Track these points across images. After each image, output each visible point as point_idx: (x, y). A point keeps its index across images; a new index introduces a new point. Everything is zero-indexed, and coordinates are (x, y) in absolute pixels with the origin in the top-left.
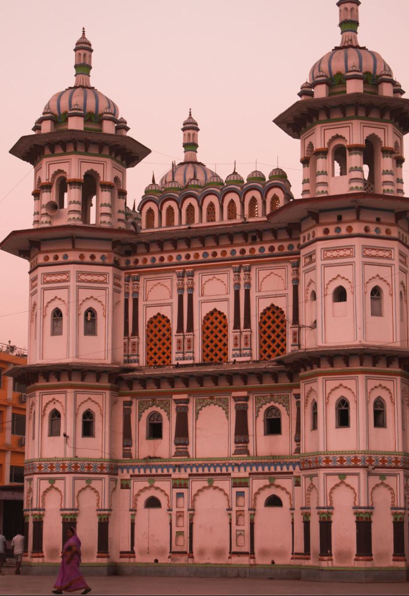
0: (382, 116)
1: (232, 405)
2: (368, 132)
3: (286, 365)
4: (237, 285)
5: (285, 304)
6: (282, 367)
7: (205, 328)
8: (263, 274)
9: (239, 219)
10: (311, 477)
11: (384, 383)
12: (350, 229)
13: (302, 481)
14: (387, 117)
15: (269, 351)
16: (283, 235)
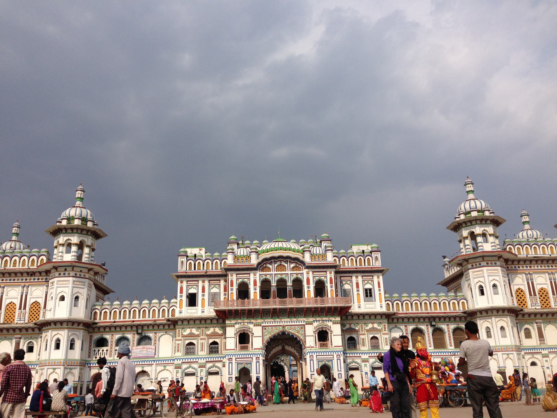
0: (87, 233)
1: (14, 341)
2: (81, 239)
3: (38, 325)
4: (22, 293)
5: (41, 301)
6: (36, 326)
7: (6, 309)
8: (34, 288)
9: (26, 267)
10: (42, 369)
11: (75, 333)
12: (69, 274)
13: (39, 371)
14: (89, 234)
15: (32, 319)
16: (44, 274)
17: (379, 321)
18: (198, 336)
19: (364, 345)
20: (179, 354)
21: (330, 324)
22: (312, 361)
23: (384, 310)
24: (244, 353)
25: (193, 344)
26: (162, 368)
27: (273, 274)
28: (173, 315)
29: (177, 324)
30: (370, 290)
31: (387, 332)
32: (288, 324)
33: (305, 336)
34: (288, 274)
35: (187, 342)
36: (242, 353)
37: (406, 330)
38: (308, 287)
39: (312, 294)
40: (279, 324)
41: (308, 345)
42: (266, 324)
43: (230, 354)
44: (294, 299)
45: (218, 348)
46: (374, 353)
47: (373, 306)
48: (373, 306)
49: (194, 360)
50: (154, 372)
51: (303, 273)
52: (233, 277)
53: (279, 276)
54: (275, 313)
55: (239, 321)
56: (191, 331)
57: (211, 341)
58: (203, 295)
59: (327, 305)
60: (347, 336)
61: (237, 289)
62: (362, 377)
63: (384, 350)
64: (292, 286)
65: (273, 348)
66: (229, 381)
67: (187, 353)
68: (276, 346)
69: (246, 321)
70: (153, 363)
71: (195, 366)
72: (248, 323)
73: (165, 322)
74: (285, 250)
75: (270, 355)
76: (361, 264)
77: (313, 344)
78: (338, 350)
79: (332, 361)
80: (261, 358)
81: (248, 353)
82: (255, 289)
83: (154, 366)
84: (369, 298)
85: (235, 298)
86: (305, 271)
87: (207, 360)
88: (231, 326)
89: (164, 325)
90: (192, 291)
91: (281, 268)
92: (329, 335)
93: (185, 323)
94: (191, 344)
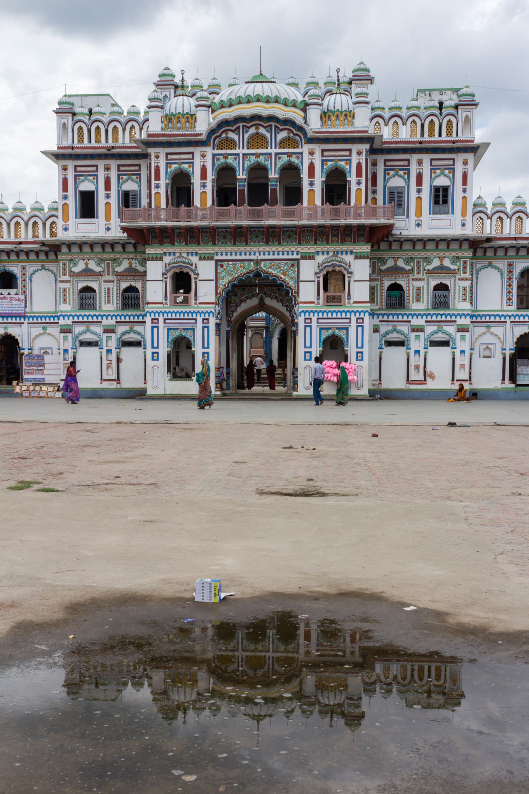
17: (454, 254)
18: (100, 274)
19: (418, 300)
20: (66, 308)
21: (348, 258)
22: (308, 329)
23: (470, 231)
24: (180, 309)
25: (93, 290)
26: (40, 330)
27: (242, 158)
28: (53, 234)
29: (60, 250)
30: (446, 189)
31: (468, 275)
32: (267, 257)
33: (298, 281)
34: (270, 154)
35: (81, 285)
36: (176, 310)
37: (510, 272)
38: (311, 184)
39: (318, 201)
40: (248, 257)
41: (301, 299)
42: (224, 257)
43: (155, 310)
44: (280, 208)
45: (138, 298)
46: (437, 315)
47: (447, 223)
48: (447, 223)
49: (95, 319)
50: (25, 338)
51: (301, 153)
52: (160, 158)
53: (253, 159)
54: (239, 235)
55: (171, 250)
56: (87, 264)
57: (125, 285)
58: (108, 196)
59: (343, 222)
60: (387, 283)
61: (167, 184)
62: (408, 360)
63: (457, 310)
64: (281, 180)
65: (241, 301)
66: (153, 359)
67: (82, 306)
68: (247, 298)
69: (184, 249)
70: (22, 320)
71: (98, 329)
72: (188, 254)
73: (35, 246)
74: (268, 102)
75: (235, 314)
76: (431, 134)
77: (312, 297)
78: (360, 310)
79: (347, 329)
80: (213, 321)
81: (188, 310)
82: (204, 186)
83: (25, 326)
84: (441, 207)
85: (163, 205)
86: (306, 149)
87: (118, 320)
88: (156, 259)
89: (37, 253)
90: (87, 186)
91: (257, 141)
92: (347, 280)
93: (75, 249)
94: (88, 289)
